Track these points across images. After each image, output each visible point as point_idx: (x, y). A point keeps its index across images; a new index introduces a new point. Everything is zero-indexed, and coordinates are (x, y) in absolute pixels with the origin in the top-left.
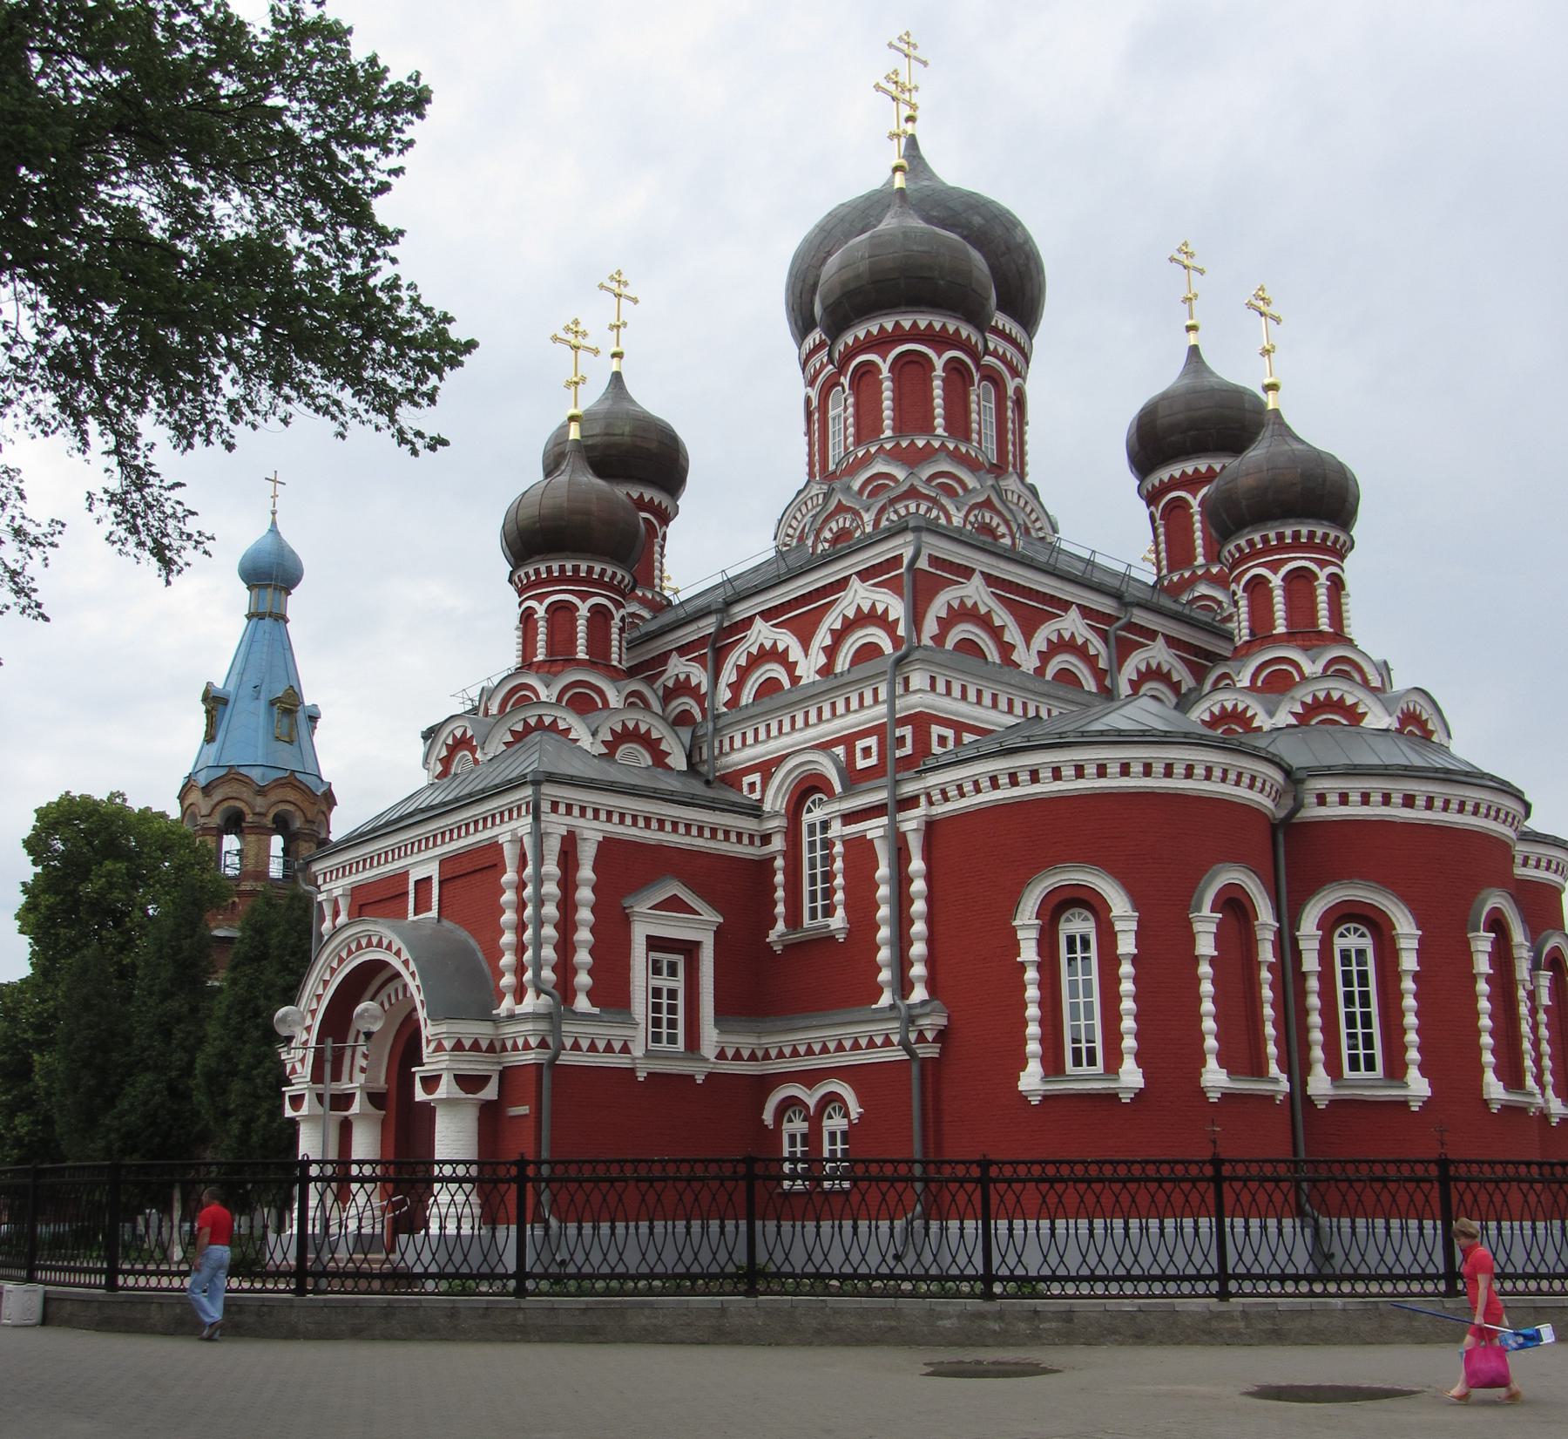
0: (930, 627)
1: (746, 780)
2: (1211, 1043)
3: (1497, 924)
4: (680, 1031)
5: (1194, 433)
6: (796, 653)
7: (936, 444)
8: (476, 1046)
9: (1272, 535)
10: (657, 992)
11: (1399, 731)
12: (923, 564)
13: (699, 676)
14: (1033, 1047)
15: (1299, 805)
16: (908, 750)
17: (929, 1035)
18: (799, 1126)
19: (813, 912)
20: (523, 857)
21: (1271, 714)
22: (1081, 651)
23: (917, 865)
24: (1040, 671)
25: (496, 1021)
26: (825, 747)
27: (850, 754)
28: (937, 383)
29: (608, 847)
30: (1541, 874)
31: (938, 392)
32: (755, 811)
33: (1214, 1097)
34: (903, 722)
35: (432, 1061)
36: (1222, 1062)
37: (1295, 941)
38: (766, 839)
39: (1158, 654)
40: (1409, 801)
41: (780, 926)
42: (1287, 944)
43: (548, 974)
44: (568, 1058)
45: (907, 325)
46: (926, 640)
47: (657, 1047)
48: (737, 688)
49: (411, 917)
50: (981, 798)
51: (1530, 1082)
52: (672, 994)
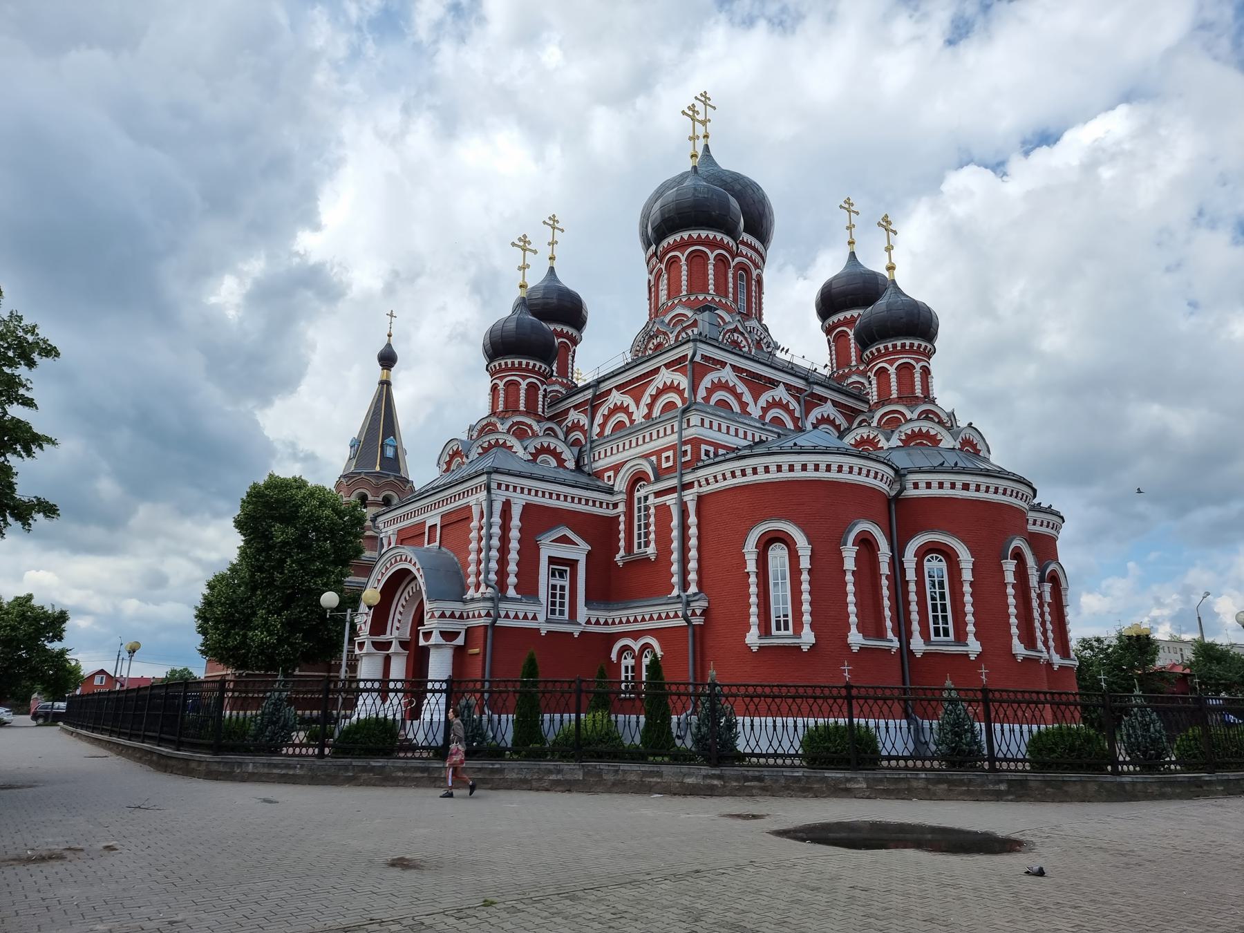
0: (702, 393)
1: (606, 475)
2: (853, 619)
3: (1018, 555)
4: (566, 609)
6: (632, 408)
7: (709, 298)
8: (452, 616)
9: (890, 345)
10: (554, 587)
11: (961, 450)
12: (698, 359)
13: (584, 420)
14: (754, 619)
15: (903, 489)
16: (688, 458)
17: (698, 612)
18: (629, 662)
19: (639, 544)
20: (482, 512)
21: (888, 440)
22: (785, 407)
23: (692, 520)
24: (762, 417)
25: (464, 602)
26: (646, 457)
27: (659, 460)
28: (711, 267)
29: (527, 508)
30: (1044, 530)
31: (711, 272)
32: (610, 491)
33: (855, 649)
34: (685, 443)
35: (430, 623)
36: (861, 628)
37: (902, 563)
38: (615, 506)
39: (828, 410)
40: (966, 487)
41: (622, 552)
43: (493, 577)
44: (501, 622)
45: (695, 236)
46: (699, 400)
47: (553, 617)
48: (603, 426)
49: (426, 546)
50: (726, 483)
51: (1040, 645)
52: (562, 588)
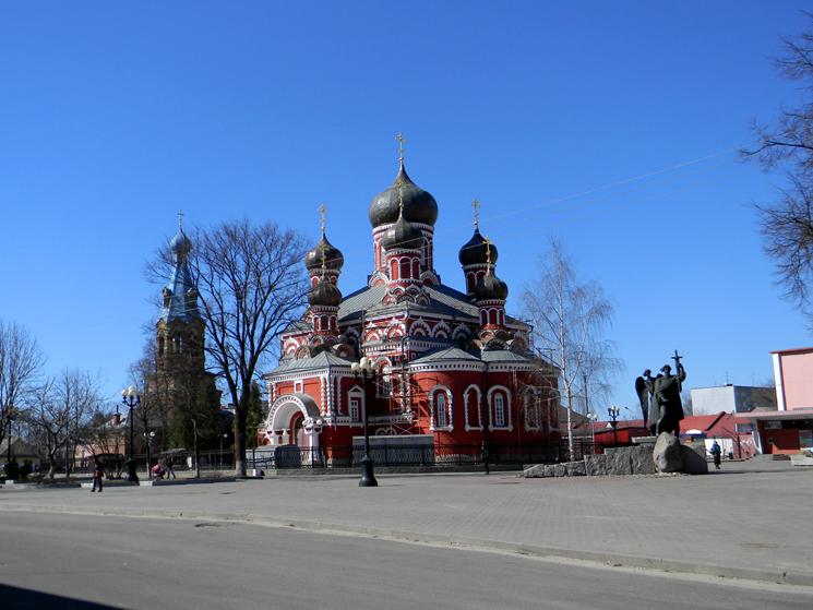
5: (476, 254)
13: (356, 332)
42: (484, 399)
